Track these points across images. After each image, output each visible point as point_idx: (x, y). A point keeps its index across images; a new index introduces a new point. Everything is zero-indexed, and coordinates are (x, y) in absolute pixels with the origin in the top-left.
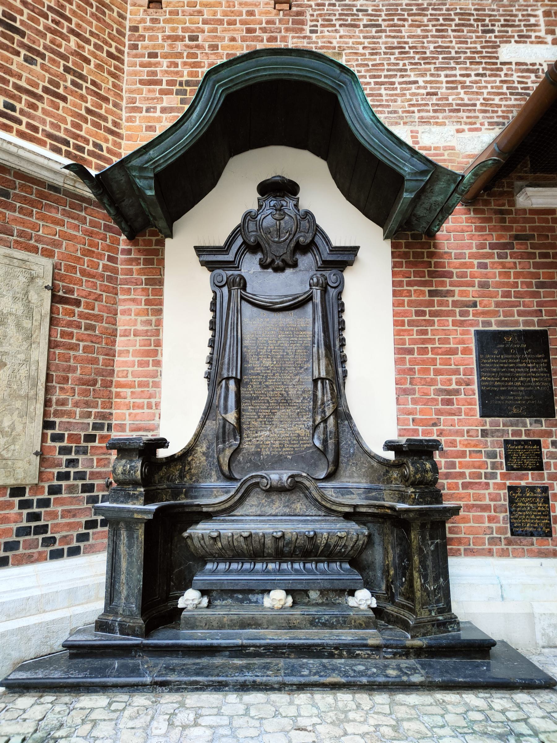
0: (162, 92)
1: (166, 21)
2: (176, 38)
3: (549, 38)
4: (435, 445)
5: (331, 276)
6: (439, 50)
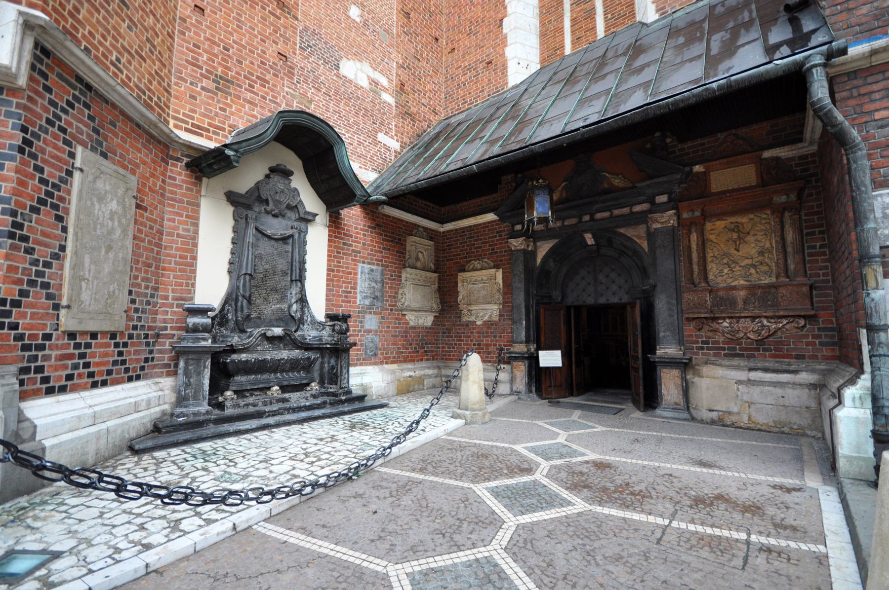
4: (349, 316)
5: (302, 225)
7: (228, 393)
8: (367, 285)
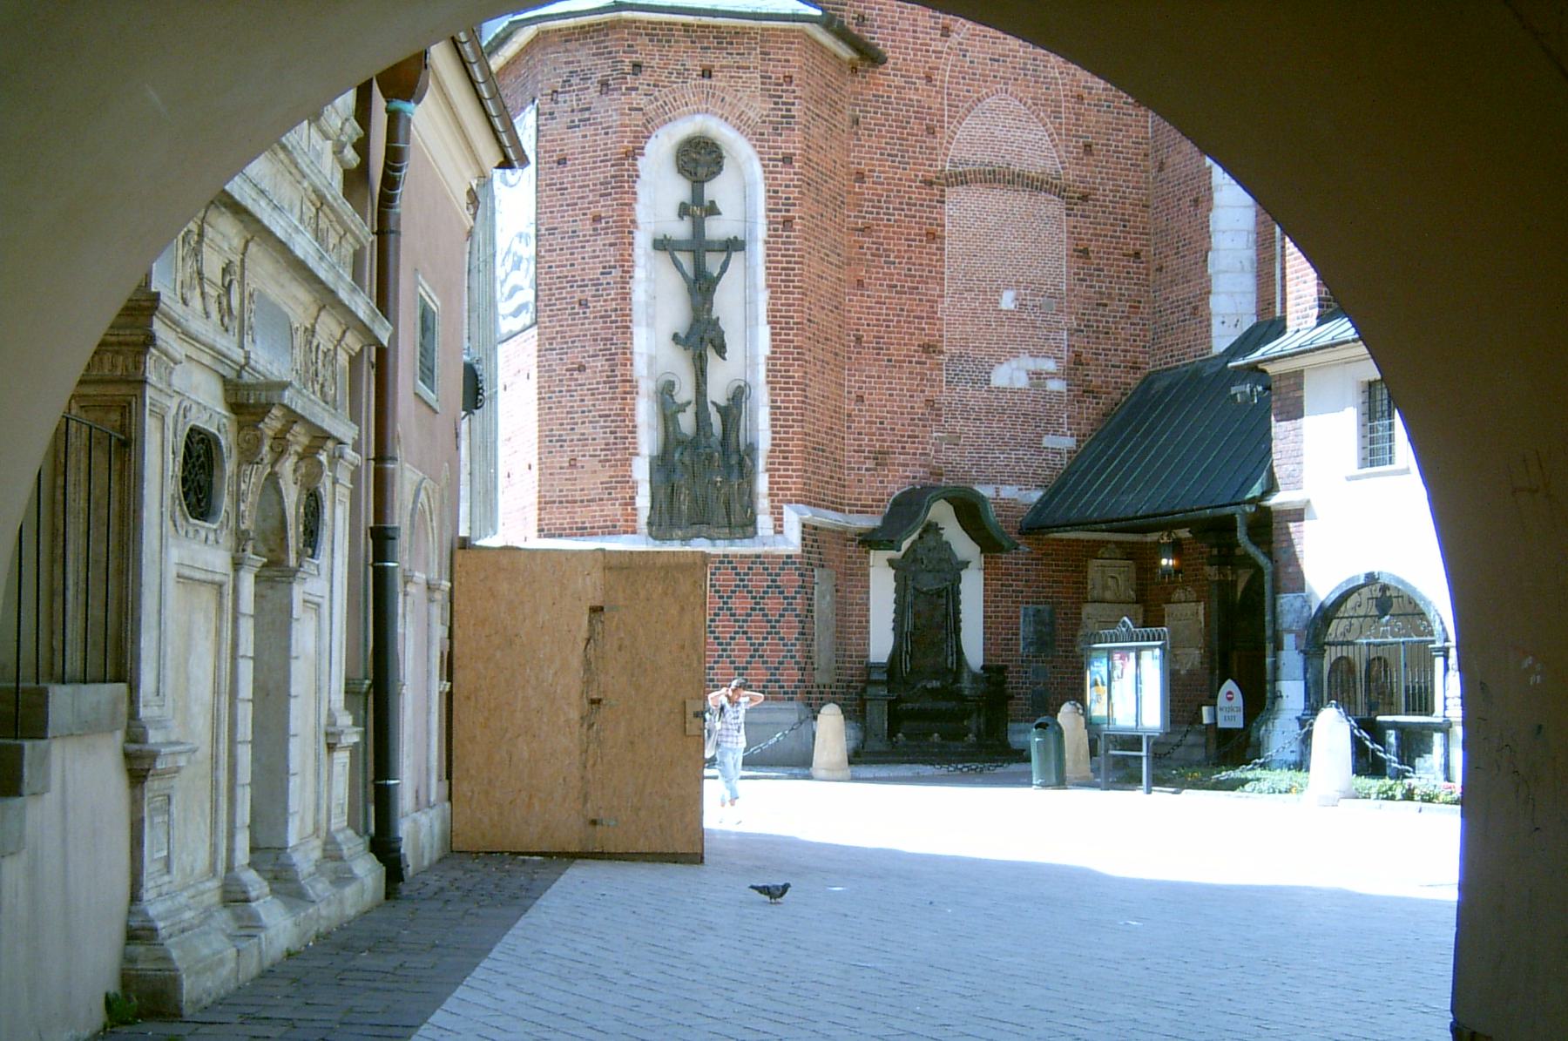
0: (865, 458)
1: (867, 411)
2: (871, 422)
3: (1069, 433)
4: (1006, 667)
6: (1013, 437)
7: (900, 735)
8: (1032, 629)
